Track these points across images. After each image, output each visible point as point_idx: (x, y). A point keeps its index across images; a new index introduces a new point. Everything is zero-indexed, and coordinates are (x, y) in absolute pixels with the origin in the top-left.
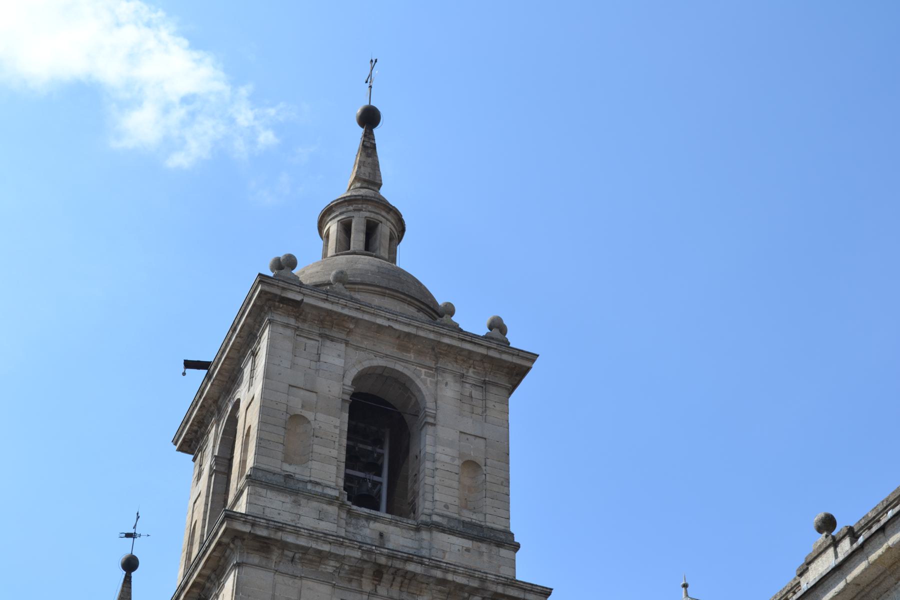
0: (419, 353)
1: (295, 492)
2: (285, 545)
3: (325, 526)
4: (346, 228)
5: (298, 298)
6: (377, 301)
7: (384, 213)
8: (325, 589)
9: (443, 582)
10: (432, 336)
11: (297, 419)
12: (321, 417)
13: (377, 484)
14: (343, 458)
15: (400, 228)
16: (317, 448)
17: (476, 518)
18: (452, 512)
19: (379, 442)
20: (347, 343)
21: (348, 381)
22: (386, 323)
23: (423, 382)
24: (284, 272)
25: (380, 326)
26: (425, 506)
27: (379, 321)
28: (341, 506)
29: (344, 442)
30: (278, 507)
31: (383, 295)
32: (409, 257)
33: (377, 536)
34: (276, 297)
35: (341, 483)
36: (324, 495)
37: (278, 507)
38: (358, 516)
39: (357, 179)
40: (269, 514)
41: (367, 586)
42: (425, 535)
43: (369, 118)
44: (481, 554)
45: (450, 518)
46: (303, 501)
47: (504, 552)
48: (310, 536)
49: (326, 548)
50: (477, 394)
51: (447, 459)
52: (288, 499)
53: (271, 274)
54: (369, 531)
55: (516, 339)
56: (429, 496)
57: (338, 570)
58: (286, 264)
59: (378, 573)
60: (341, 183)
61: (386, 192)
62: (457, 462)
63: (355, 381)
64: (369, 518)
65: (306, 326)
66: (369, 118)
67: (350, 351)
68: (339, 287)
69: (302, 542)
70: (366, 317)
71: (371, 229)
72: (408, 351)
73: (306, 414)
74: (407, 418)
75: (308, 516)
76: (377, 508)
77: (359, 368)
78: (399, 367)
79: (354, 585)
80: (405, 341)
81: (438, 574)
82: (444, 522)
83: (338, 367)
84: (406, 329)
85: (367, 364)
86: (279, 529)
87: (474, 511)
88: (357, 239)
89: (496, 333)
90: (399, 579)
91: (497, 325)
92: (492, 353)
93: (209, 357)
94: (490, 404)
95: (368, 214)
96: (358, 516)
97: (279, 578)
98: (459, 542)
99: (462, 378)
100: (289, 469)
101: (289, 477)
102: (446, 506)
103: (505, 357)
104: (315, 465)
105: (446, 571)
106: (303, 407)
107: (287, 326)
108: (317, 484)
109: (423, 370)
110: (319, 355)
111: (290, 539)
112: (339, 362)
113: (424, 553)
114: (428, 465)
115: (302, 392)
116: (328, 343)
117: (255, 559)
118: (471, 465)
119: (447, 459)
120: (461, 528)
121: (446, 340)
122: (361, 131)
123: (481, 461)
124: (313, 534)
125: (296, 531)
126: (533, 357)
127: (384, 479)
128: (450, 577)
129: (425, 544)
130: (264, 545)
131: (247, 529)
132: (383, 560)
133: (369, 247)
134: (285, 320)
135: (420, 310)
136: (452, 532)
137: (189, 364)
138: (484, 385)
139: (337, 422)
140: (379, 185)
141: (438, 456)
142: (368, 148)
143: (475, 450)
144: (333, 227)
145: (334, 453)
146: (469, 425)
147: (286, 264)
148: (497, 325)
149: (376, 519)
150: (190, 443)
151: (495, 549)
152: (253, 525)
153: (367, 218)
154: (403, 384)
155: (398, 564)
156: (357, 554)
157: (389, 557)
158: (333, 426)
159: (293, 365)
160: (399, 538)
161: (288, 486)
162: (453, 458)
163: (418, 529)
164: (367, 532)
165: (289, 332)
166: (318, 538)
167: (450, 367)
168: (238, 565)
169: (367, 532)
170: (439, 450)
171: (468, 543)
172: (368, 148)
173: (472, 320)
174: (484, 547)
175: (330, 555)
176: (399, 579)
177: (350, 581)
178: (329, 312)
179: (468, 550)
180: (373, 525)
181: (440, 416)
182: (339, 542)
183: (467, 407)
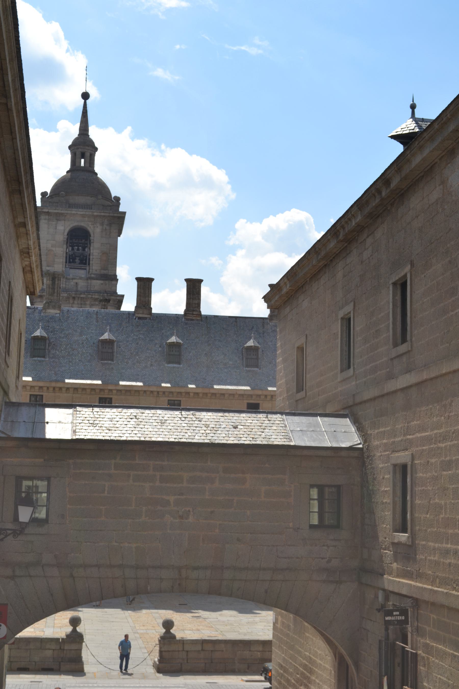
5: (47, 211)
7: (87, 148)
16: (56, 260)
20: (65, 220)
21: (66, 234)
22: (75, 212)
25: (74, 214)
41: (71, 301)
42: (89, 281)
47: (113, 282)
50: (108, 228)
79: (68, 302)
85: (72, 226)
95: (80, 150)
99: (102, 224)
102: (96, 271)
106: (52, 246)
107: (45, 219)
109: (90, 223)
110: (56, 227)
122: (83, 101)
136: (97, 279)
141: (94, 254)
164: (72, 283)
165: (46, 221)
169: (72, 283)
170: (95, 251)
171: (102, 282)
177: (66, 301)
179: (102, 284)
180: (74, 281)
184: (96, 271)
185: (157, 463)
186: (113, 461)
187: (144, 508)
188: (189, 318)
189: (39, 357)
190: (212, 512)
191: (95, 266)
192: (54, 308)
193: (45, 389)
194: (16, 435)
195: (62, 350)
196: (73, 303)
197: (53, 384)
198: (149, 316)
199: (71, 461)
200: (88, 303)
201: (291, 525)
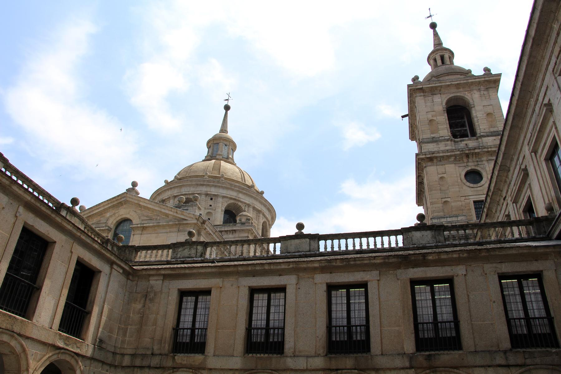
0: (463, 88)
1: (436, 141)
2: (436, 157)
3: (448, 148)
4: (435, 60)
5: (421, 87)
6: (447, 78)
8: (453, 165)
9: (488, 152)
10: (465, 81)
11: (431, 121)
12: (438, 118)
13: (466, 130)
14: (448, 126)
15: (452, 54)
17: (495, 129)
18: (487, 130)
19: (463, 118)
21: (444, 104)
22: (450, 83)
23: (467, 96)
24: (416, 81)
25: (448, 85)
26: (478, 131)
27: (448, 84)
28: (451, 140)
29: (448, 122)
30: (431, 147)
31: (448, 75)
32: (458, 62)
33: (465, 145)
34: (416, 90)
35: (450, 134)
36: (445, 139)
37: (431, 147)
38: (458, 142)
39: (434, 45)
40: (430, 150)
41: (465, 160)
42: (480, 140)
43: (433, 26)
46: (439, 143)
48: (443, 152)
49: (449, 154)
50: (485, 93)
52: (435, 144)
53: (412, 83)
54: (462, 145)
55: (493, 72)
56: (478, 128)
57: (455, 159)
58: (416, 79)
59: (467, 156)
60: (431, 48)
61: (445, 45)
63: (447, 103)
64: (461, 141)
65: (427, 94)
66: (433, 26)
67: (442, 96)
68: (434, 78)
69: (441, 155)
70: (443, 84)
71: (442, 58)
72: (460, 88)
73: (433, 118)
74: (467, 108)
75: (442, 147)
76: (467, 137)
77: (446, 99)
78: (458, 94)
79: (461, 161)
80: (458, 86)
81: (486, 150)
82: (485, 134)
83: (439, 102)
84: (456, 83)
85: (448, 97)
86: (433, 153)
87: (494, 127)
88: (439, 62)
89: (487, 72)
90: (474, 155)
91: (487, 70)
92: (487, 79)
93: (407, 113)
94: (490, 94)
96: (458, 142)
97: (438, 167)
98: (491, 138)
99: (479, 90)
103: (490, 78)
104: (440, 132)
105: (488, 148)
107: (421, 96)
111: (438, 155)
112: (440, 100)
113: (481, 145)
114: (475, 119)
116: (435, 96)
117: (429, 164)
120: (490, 134)
121: (470, 81)
123: (492, 112)
124: (443, 152)
125: (438, 152)
126: (500, 75)
127: (467, 128)
128: (490, 150)
129: (481, 143)
130: (431, 159)
131: (424, 156)
132: (467, 152)
133: (443, 62)
134: (420, 94)
135: (461, 75)
136: (488, 136)
137: (403, 117)
138: (487, 89)
139: (444, 117)
140: (442, 44)
142: (436, 35)
143: (489, 109)
144: (432, 62)
145: (445, 126)
146: (485, 103)
147: (416, 79)
148: (487, 70)
149: (463, 141)
150: (413, 137)
152: (425, 155)
153: (441, 56)
154: (462, 99)
155: (472, 151)
156: (458, 153)
157: (469, 150)
158: (443, 119)
159: (426, 106)
160: (471, 143)
161: (434, 140)
163: (477, 139)
164: (462, 145)
165: (422, 97)
166: (445, 152)
167: (474, 88)
168: (425, 167)
169: (462, 145)
171: (494, 138)
172: (436, 35)
173: (478, 71)
175: (451, 156)
176: (474, 155)
178: (432, 87)
180: (463, 142)
181: (475, 104)
182: (452, 151)
183: (483, 98)
196: (468, 162)
200: (484, 158)
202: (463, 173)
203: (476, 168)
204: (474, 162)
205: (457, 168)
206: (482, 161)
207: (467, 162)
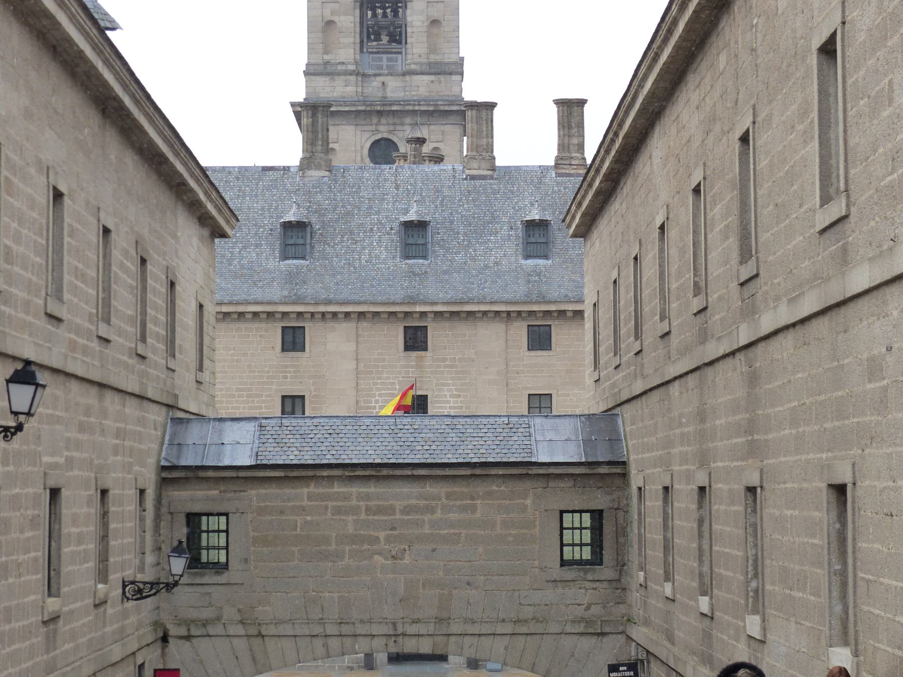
11: (330, 23)
44: (440, 82)
45: (421, 64)
47: (455, 78)
51: (419, 23)
52: (327, 79)
62: (426, 24)
100: (327, 57)
101: (327, 63)
108: (343, 63)
115: (330, 5)
118: (435, 22)
119: (419, 23)
139: (351, 18)
151: (448, 77)
162: (423, 22)
169: (375, 84)
171: (432, 78)
174: (442, 77)
179: (432, 82)
184: (420, 56)
185: (361, 490)
186: (306, 490)
187: (347, 548)
188: (563, 171)
189: (295, 258)
190: (434, 550)
191: (417, 47)
192: (318, 167)
193: (309, 316)
194: (183, 463)
195: (335, 244)
197: (322, 309)
198: (490, 172)
199: (253, 492)
201: (536, 563)
202: (368, 145)
203: (391, 137)
204: (388, 124)
205: (358, 133)
206: (403, 125)
207: (376, 125)
